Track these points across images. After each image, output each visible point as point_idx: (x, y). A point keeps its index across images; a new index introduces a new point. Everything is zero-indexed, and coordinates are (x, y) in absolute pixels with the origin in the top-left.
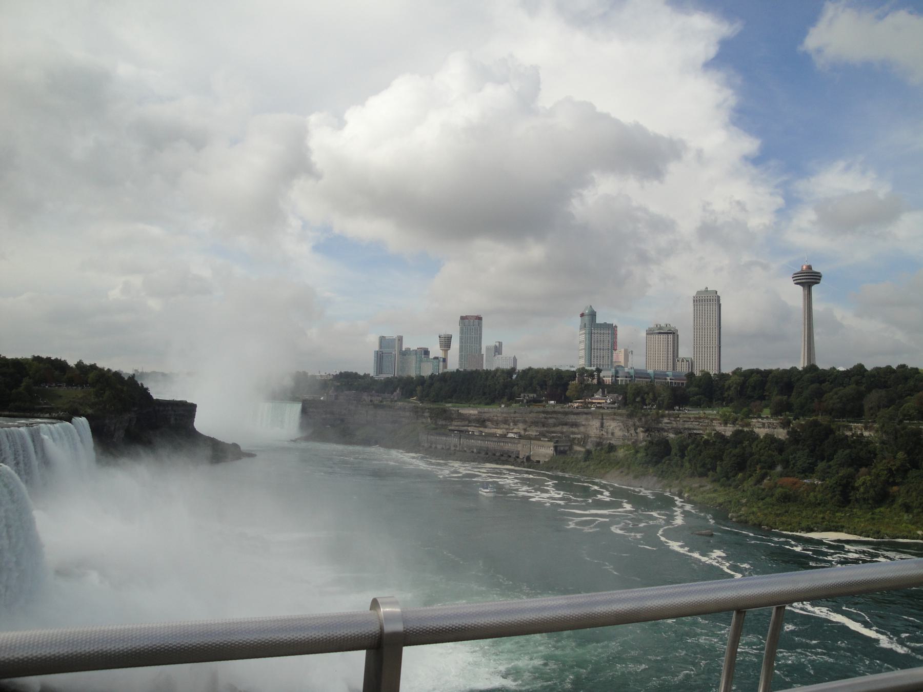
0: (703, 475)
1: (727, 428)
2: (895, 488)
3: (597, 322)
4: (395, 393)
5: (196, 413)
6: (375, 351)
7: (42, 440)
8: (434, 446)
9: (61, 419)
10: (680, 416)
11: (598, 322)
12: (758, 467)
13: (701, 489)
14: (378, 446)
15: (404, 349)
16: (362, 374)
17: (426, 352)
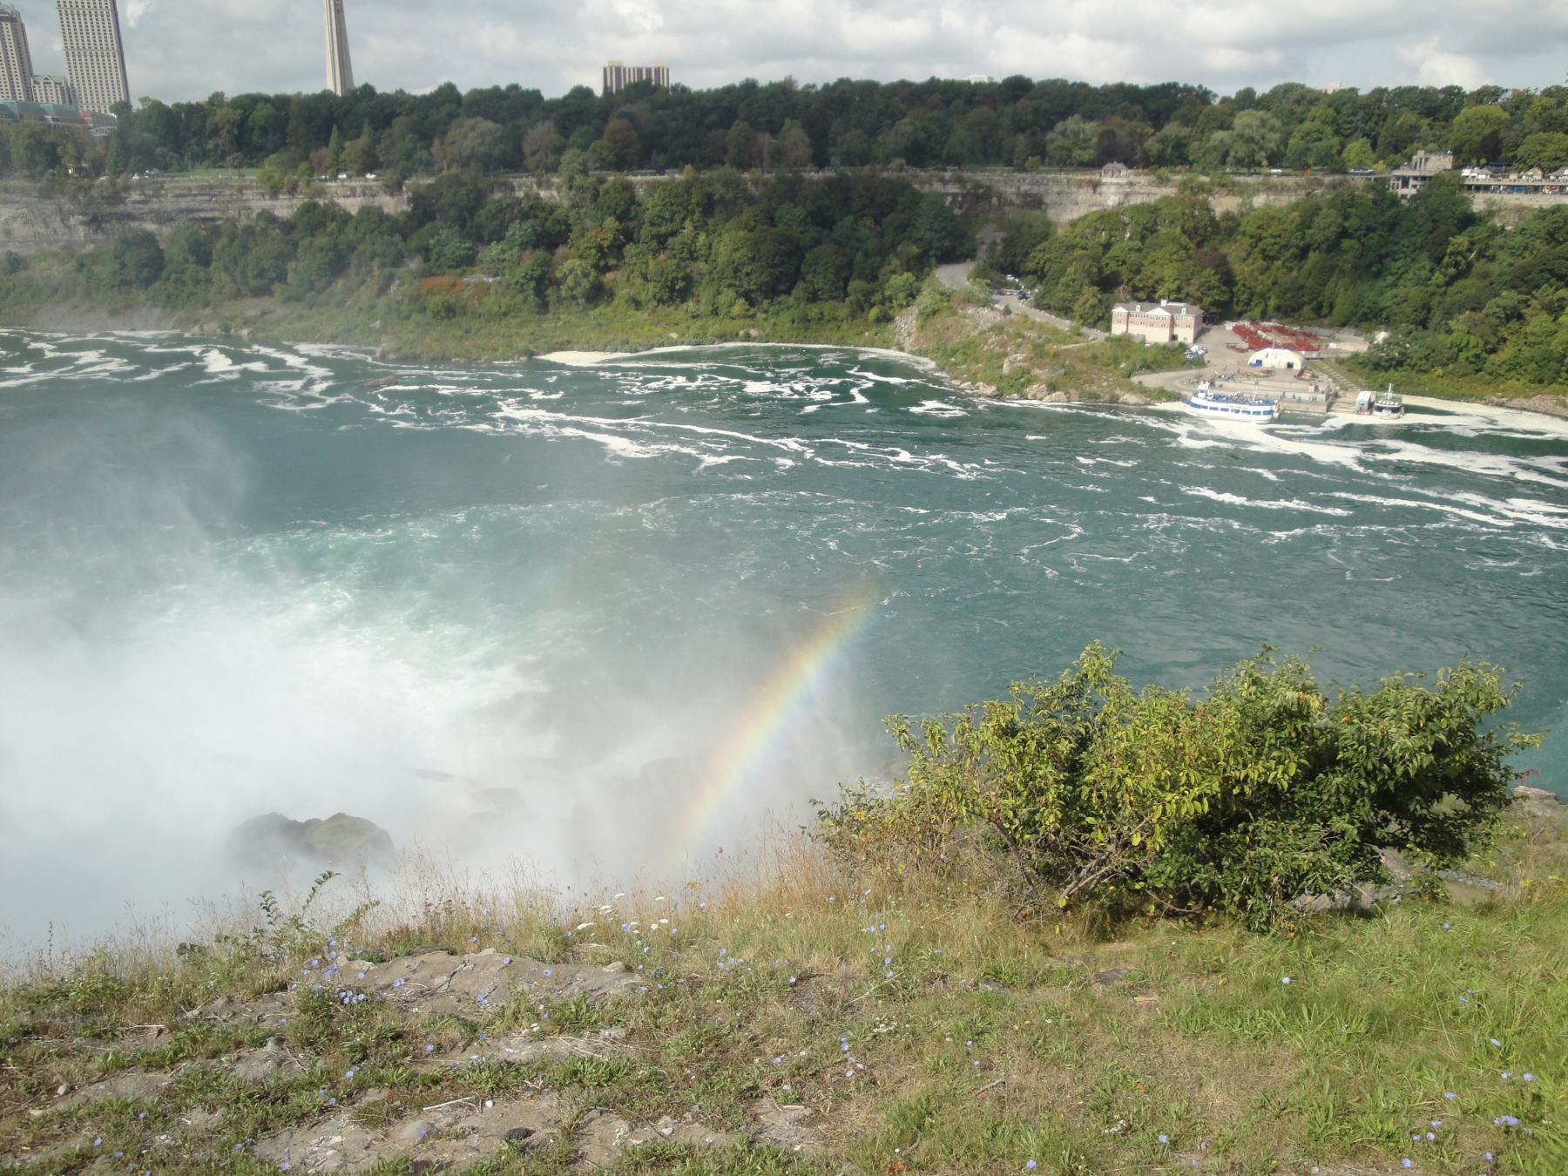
0: (262, 291)
1: (278, 203)
2: (610, 276)
10: (166, 186)
12: (375, 264)
13: (267, 317)
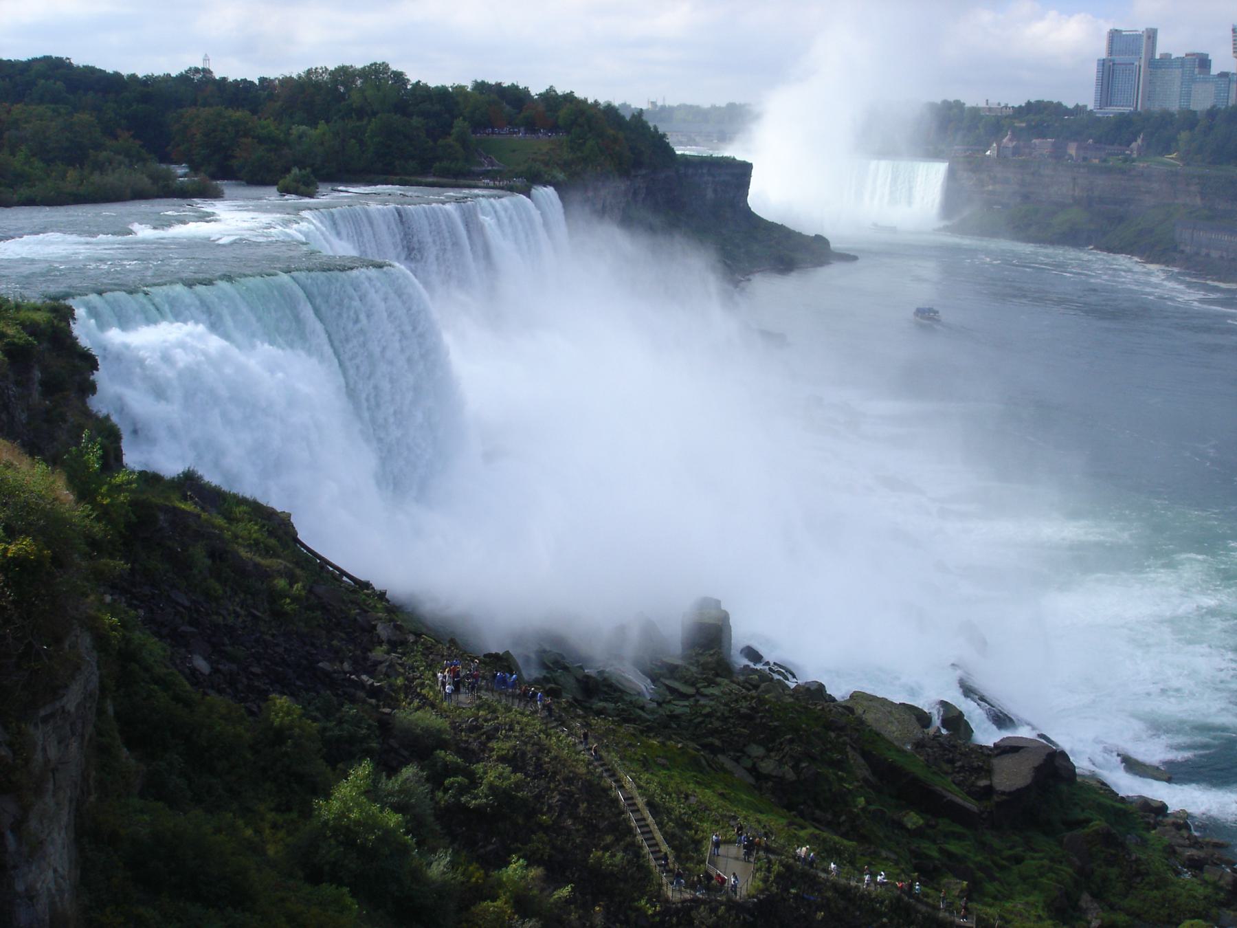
4: (1134, 145)
5: (752, 178)
6: (1099, 60)
7: (481, 229)
8: (1204, 251)
9: (512, 189)
14: (1091, 247)
15: (1157, 57)
16: (1071, 105)
17: (1204, 62)
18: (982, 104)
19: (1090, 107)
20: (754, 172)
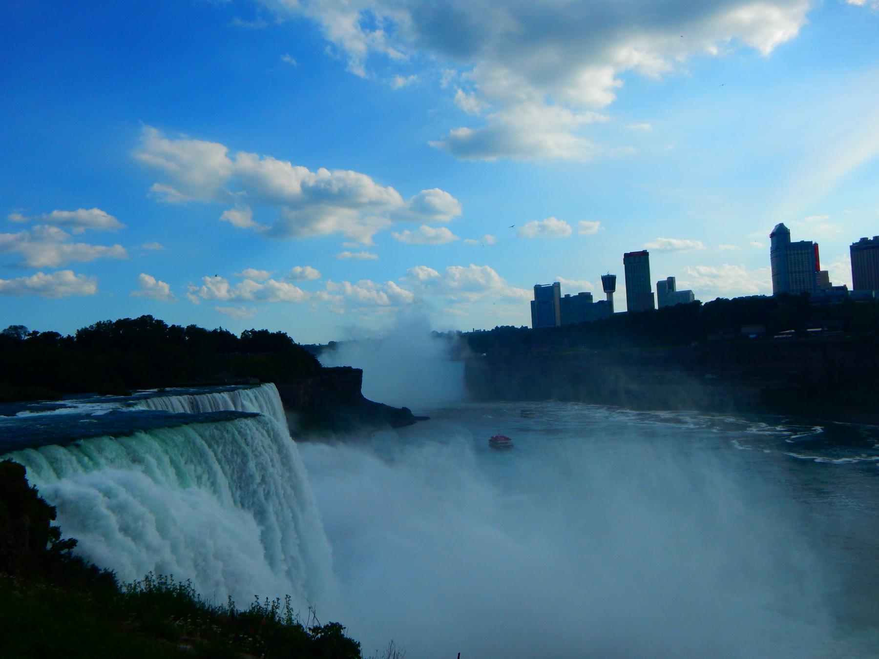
3: (792, 241)
6: (531, 302)
11: (792, 241)
15: (563, 296)
18: (472, 331)
19: (530, 326)
20: (363, 374)
